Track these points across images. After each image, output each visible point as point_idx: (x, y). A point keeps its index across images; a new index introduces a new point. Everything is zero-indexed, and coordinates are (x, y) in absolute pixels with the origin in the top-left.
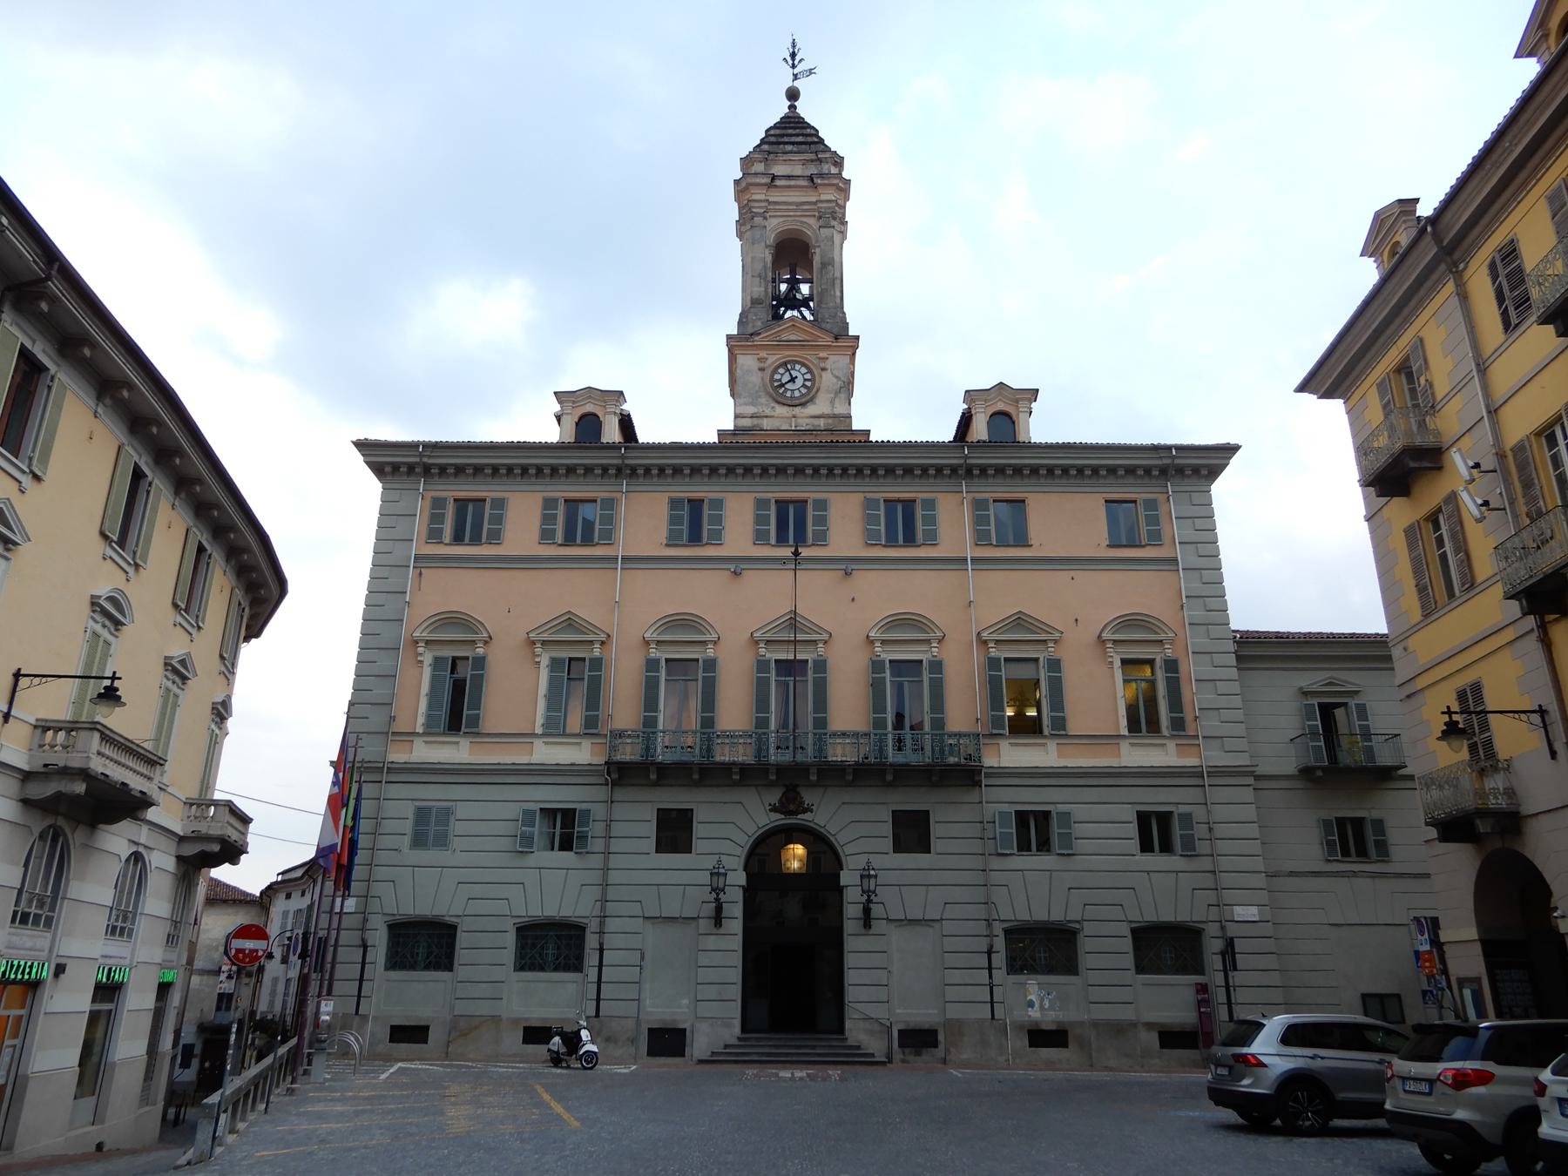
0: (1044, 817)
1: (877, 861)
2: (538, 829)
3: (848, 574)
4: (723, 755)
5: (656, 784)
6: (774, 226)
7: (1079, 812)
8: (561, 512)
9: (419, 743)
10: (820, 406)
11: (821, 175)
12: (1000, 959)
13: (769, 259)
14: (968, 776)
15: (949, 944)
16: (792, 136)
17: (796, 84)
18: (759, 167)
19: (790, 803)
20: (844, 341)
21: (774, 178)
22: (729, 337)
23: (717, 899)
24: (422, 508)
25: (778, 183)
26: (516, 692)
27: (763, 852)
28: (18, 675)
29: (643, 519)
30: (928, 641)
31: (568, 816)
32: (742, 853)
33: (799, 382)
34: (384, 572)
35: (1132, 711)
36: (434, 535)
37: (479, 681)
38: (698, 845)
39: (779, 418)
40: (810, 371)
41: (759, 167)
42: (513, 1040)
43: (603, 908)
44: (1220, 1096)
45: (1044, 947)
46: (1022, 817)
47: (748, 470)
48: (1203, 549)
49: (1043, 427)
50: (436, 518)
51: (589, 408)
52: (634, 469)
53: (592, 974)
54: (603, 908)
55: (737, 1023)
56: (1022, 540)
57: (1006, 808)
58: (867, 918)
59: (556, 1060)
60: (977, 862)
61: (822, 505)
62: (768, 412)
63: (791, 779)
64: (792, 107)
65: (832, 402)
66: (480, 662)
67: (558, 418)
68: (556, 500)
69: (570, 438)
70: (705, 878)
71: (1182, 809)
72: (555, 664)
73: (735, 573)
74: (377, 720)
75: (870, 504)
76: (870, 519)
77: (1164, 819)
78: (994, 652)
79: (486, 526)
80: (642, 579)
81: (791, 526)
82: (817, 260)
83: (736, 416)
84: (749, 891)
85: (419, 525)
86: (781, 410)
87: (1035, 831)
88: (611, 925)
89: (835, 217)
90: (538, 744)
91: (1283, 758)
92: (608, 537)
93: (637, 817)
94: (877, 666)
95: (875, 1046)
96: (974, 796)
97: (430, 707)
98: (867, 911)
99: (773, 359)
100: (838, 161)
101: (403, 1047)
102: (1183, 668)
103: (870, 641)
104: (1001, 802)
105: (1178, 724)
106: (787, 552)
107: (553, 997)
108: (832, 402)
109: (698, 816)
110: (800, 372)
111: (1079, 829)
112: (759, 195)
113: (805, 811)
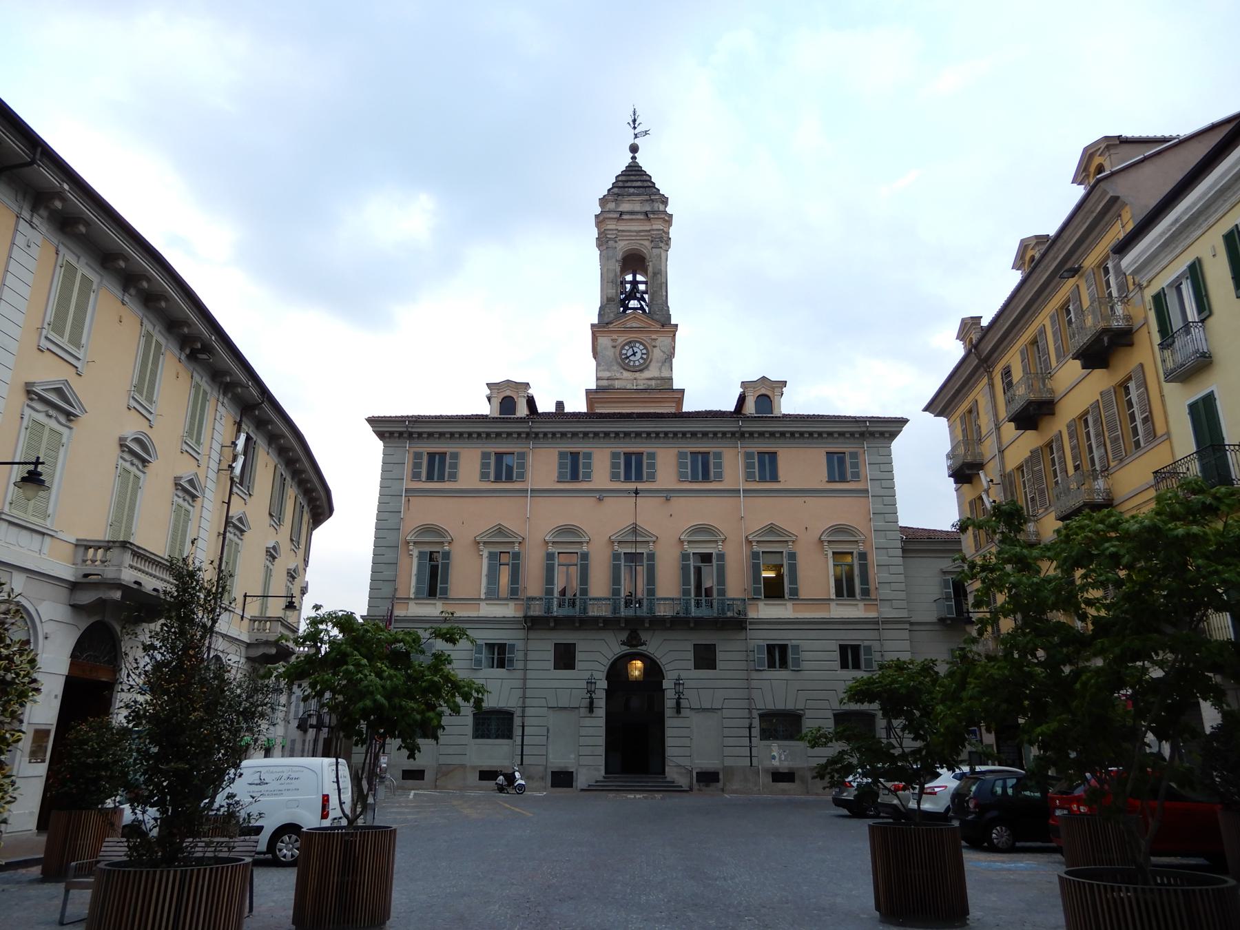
0: (783, 648)
1: (684, 674)
2: (484, 656)
3: (668, 499)
4: (593, 612)
5: (553, 629)
6: (622, 246)
7: (805, 645)
8: (493, 460)
9: (412, 604)
10: (652, 372)
11: (653, 212)
12: (756, 732)
13: (618, 269)
14: (739, 624)
15: (727, 723)
16: (634, 184)
17: (637, 141)
18: (612, 206)
19: (633, 640)
20: (667, 327)
21: (622, 213)
22: (593, 326)
23: (591, 698)
24: (408, 459)
25: (624, 217)
26: (468, 574)
27: (616, 671)
28: (245, 596)
29: (543, 465)
30: (716, 542)
31: (502, 647)
32: (605, 669)
33: (639, 355)
34: (387, 499)
35: (838, 582)
36: (416, 476)
37: (446, 567)
38: (578, 665)
39: (625, 379)
40: (646, 348)
41: (612, 206)
42: (474, 778)
43: (524, 702)
44: (839, 802)
45: (780, 725)
46: (771, 648)
47: (607, 434)
48: (885, 484)
49: (789, 404)
50: (417, 465)
51: (508, 393)
52: (537, 434)
53: (519, 740)
54: (524, 702)
55: (603, 768)
56: (774, 478)
57: (761, 643)
58: (678, 708)
59: (501, 789)
60: (743, 675)
61: (652, 456)
62: (618, 375)
63: (634, 625)
64: (634, 158)
65: (660, 369)
66: (447, 555)
67: (489, 399)
68: (489, 454)
69: (497, 415)
70: (583, 684)
71: (867, 643)
72: (492, 556)
73: (600, 499)
74: (386, 590)
75: (681, 455)
76: (682, 465)
77: (855, 649)
78: (756, 548)
79: (447, 470)
80: (545, 503)
81: (633, 468)
82: (650, 270)
83: (598, 379)
84: (609, 693)
85: (407, 470)
86: (626, 374)
87: (779, 656)
88: (529, 712)
89: (663, 241)
90: (483, 604)
91: (928, 611)
92: (522, 476)
93: (543, 648)
94: (685, 557)
95: (683, 782)
96: (742, 635)
97: (418, 581)
98: (678, 704)
99: (621, 339)
100: (664, 201)
101: (410, 782)
102: (869, 557)
103: (681, 542)
104: (759, 639)
105: (866, 592)
106: (631, 486)
107: (496, 753)
108: (660, 369)
109: (578, 648)
110: (639, 349)
111: (805, 655)
112: (611, 225)
113: (642, 644)
